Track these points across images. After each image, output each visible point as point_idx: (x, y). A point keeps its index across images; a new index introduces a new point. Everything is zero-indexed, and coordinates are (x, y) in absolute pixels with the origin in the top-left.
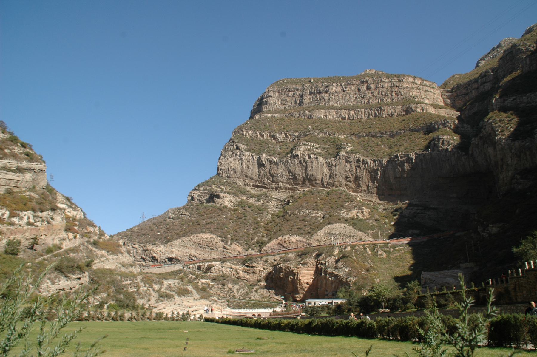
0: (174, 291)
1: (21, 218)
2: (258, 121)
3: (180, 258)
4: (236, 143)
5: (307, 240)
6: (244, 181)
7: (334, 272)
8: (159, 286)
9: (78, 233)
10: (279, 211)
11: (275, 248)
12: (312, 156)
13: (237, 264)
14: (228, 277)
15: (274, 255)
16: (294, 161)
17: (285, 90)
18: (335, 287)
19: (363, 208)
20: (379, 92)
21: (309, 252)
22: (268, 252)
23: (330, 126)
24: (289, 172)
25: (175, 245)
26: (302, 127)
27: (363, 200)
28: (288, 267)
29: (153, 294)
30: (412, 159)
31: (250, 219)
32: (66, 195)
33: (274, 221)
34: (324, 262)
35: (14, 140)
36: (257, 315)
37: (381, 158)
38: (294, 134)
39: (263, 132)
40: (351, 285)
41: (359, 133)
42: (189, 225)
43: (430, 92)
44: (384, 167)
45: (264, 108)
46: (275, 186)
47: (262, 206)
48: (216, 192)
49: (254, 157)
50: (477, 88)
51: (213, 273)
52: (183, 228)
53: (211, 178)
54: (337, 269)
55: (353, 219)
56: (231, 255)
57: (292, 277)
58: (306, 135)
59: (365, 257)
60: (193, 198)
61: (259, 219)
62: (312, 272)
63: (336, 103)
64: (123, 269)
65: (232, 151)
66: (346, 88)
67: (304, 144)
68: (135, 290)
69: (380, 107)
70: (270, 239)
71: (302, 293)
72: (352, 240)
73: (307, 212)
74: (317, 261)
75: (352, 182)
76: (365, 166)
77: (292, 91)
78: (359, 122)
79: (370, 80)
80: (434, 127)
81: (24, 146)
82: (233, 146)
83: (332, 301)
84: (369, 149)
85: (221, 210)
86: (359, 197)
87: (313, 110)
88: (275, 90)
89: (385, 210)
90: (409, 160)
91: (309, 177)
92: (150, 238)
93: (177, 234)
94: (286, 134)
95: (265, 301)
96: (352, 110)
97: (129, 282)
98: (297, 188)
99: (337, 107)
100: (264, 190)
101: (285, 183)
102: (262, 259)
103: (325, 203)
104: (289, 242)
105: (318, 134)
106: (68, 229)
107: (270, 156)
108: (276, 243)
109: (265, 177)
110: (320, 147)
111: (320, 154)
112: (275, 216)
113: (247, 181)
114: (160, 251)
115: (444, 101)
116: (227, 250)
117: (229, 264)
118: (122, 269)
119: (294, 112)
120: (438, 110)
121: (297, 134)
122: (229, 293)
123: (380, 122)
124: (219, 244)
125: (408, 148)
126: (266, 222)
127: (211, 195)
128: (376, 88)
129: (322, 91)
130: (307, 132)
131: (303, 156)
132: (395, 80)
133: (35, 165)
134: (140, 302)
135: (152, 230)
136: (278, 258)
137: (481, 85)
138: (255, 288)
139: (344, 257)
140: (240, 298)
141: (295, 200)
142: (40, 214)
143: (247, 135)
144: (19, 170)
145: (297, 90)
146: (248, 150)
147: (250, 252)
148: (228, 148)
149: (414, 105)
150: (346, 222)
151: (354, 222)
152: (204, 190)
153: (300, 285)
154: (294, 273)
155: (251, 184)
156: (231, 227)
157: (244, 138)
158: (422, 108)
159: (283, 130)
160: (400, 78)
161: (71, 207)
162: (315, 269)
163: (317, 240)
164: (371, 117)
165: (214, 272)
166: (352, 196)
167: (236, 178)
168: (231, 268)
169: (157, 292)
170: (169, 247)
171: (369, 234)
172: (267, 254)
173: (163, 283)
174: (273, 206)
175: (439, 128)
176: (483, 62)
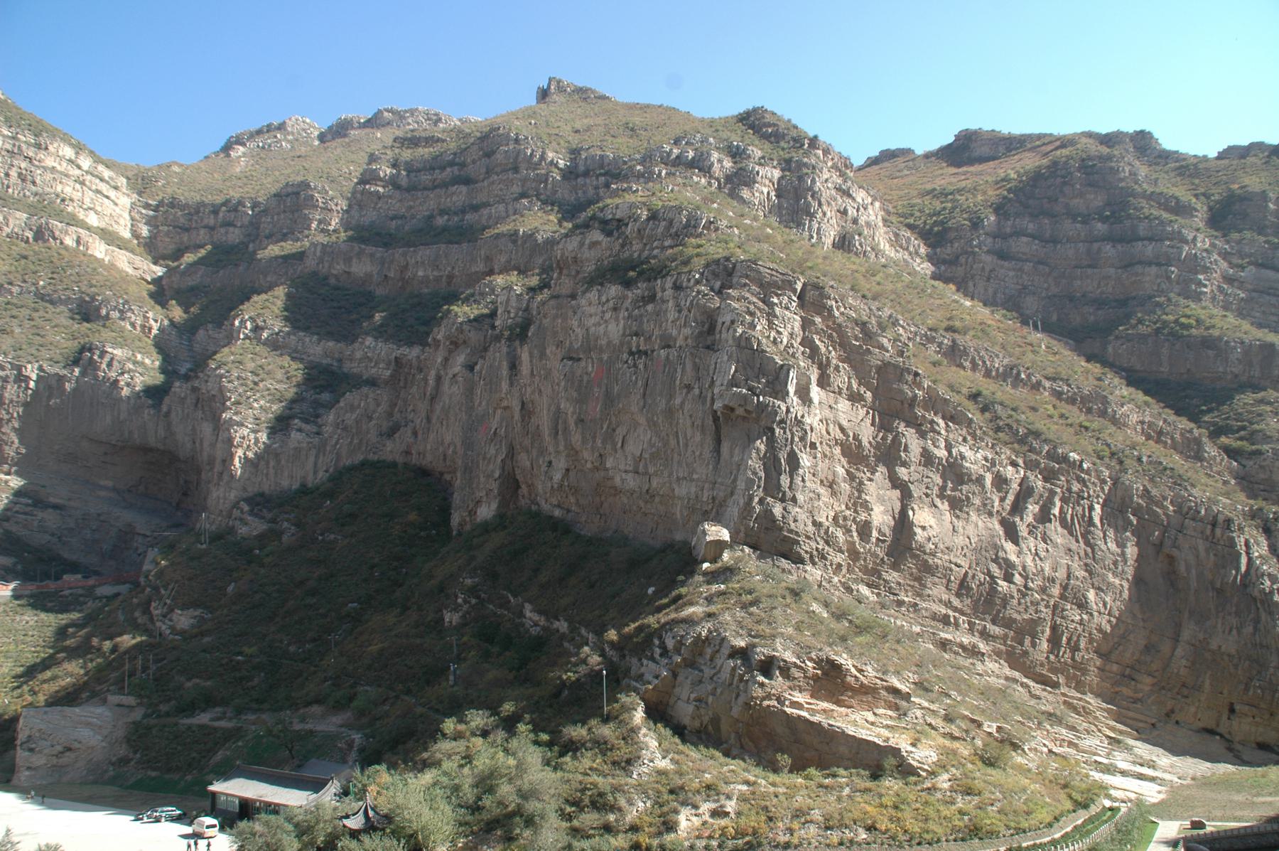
30: (28, 378)
43: (107, 197)
50: (212, 229)
80: (98, 309)
90: (21, 379)
115: (132, 225)
120: (113, 251)
125: (24, 347)
137: (221, 226)
158: (79, 237)
175: (107, 317)
176: (241, 149)
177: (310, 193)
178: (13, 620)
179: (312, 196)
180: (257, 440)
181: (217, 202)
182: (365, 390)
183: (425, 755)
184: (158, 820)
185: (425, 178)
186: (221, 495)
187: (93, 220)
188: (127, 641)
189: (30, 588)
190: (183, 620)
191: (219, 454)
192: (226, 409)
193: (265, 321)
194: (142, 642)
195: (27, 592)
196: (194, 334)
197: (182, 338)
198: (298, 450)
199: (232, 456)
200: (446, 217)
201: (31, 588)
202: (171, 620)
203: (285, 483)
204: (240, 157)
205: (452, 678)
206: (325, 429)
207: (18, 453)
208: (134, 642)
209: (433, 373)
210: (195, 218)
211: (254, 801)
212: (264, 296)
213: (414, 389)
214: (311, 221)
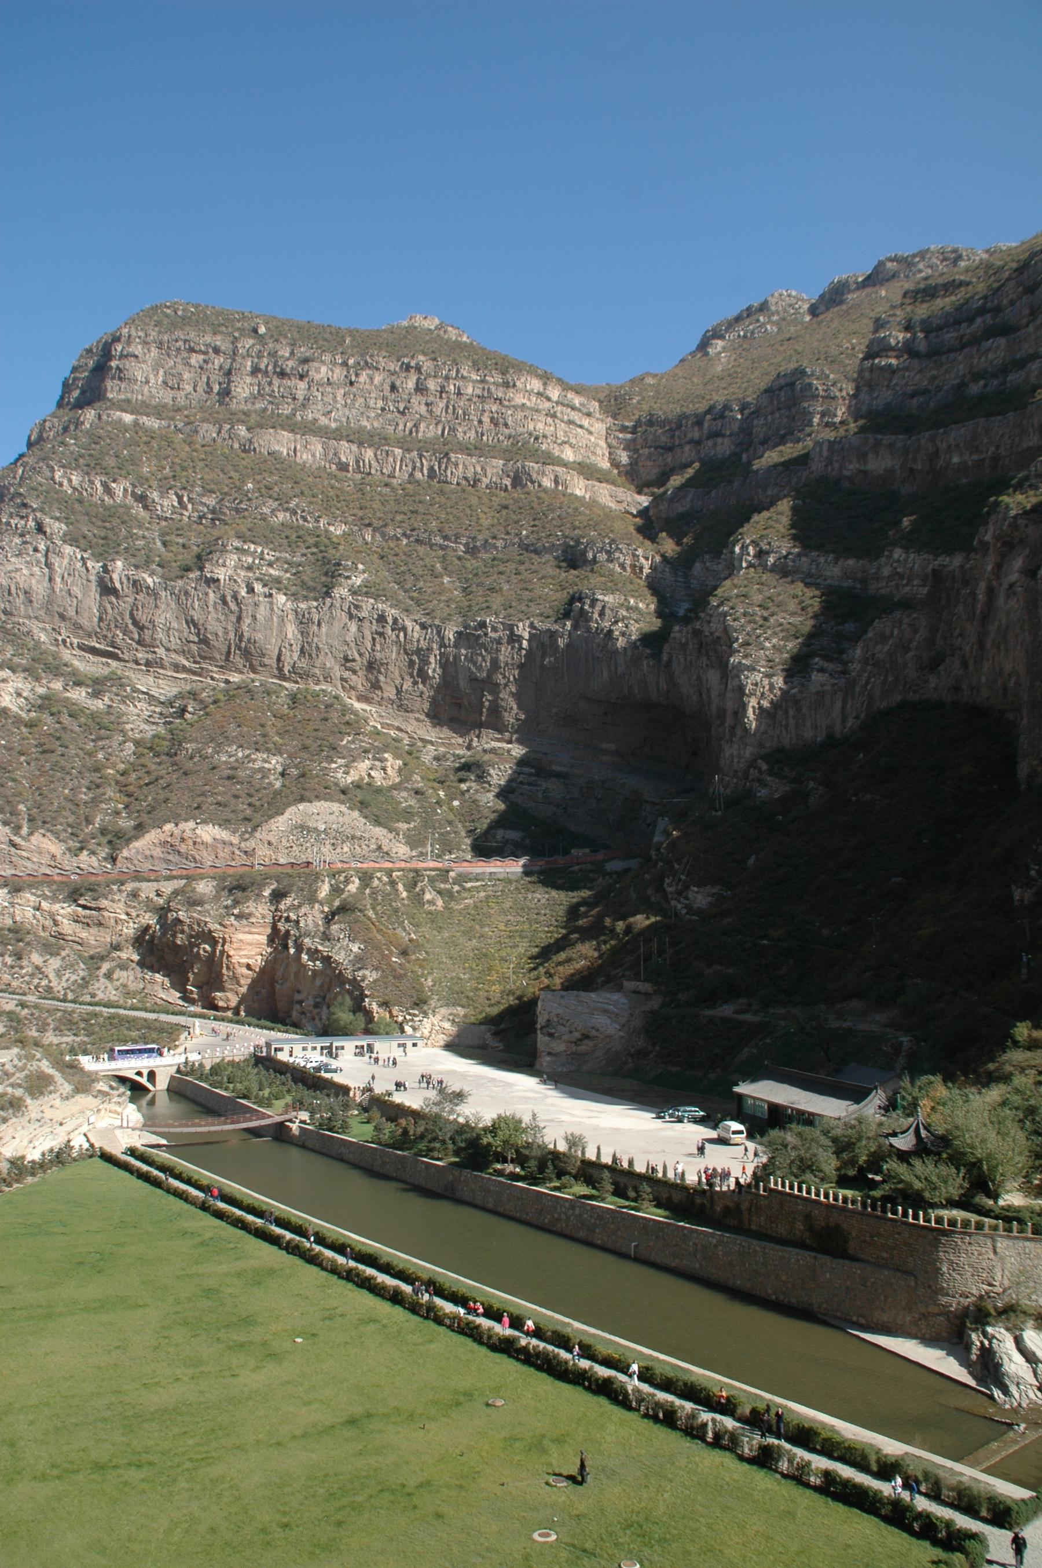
2: (95, 438)
4: (34, 510)
7: (320, 948)
11: (155, 854)
12: (258, 587)
13: (54, 899)
14: (29, 933)
16: (207, 594)
17: (180, 343)
18: (322, 986)
19: (386, 755)
20: (447, 407)
21: (253, 884)
23: (306, 491)
24: (187, 622)
26: (227, 481)
30: (520, 638)
31: (77, 755)
33: (143, 766)
34: (293, 916)
37: (443, 621)
39: (114, 481)
41: (386, 525)
43: (581, 427)
45: (112, 390)
46: (146, 656)
47: (109, 713)
49: (90, 564)
50: (697, 443)
54: (329, 940)
55: (358, 786)
57: (207, 947)
59: (396, 910)
61: (100, 756)
62: (263, 939)
65: (22, 535)
66: (357, 375)
67: (237, 549)
69: (447, 454)
70: (140, 829)
71: (232, 990)
73: (240, 754)
74: (276, 910)
76: (398, 636)
77: (201, 352)
78: (386, 485)
79: (427, 365)
80: (584, 553)
88: (149, 339)
89: (437, 758)
90: (514, 639)
91: (243, 645)
94: (180, 499)
96: (370, 446)
98: (208, 670)
99: (327, 427)
100: (114, 664)
102: (123, 888)
104: (195, 843)
107: (137, 567)
109: (116, 626)
110: (278, 559)
113: (63, 631)
115: (610, 453)
116: (19, 852)
117: (32, 898)
120: (593, 486)
121: (211, 501)
122: (36, 981)
123: (443, 500)
125: (514, 604)
126: (122, 766)
128: (441, 392)
129: (288, 370)
130: (241, 502)
136: (168, 888)
137: (708, 438)
138: (106, 966)
139: (343, 909)
140: (65, 995)
143: (65, 483)
145: (217, 351)
146: (71, 539)
149: (536, 466)
150: (342, 797)
153: (228, 968)
154: (214, 937)
155: (75, 641)
156: (24, 777)
157: (57, 492)
158: (556, 477)
162: (269, 931)
163: (270, 843)
164: (418, 475)
166: (355, 713)
167: (30, 618)
168: (38, 910)
172: (138, 877)
175: (594, 560)
176: (720, 344)
177: (807, 381)
178: (525, 898)
179: (810, 385)
180: (772, 687)
181: (700, 410)
182: (898, 614)
183: (991, 1066)
184: (680, 1120)
185: (949, 336)
186: (735, 753)
187: (569, 455)
188: (641, 921)
189: (540, 863)
190: (700, 898)
191: (730, 705)
192: (733, 652)
193: (769, 544)
194: (656, 922)
195: (537, 868)
196: (690, 568)
197: (676, 575)
198: (821, 694)
199: (744, 706)
200: (982, 383)
201: (540, 864)
202: (687, 898)
203: (808, 735)
204: (720, 353)
205: (1024, 971)
206: (851, 666)
207: (518, 720)
208: (647, 922)
209: (982, 585)
210: (677, 433)
211: (785, 1108)
212: (765, 514)
213: (960, 608)
214: (812, 414)
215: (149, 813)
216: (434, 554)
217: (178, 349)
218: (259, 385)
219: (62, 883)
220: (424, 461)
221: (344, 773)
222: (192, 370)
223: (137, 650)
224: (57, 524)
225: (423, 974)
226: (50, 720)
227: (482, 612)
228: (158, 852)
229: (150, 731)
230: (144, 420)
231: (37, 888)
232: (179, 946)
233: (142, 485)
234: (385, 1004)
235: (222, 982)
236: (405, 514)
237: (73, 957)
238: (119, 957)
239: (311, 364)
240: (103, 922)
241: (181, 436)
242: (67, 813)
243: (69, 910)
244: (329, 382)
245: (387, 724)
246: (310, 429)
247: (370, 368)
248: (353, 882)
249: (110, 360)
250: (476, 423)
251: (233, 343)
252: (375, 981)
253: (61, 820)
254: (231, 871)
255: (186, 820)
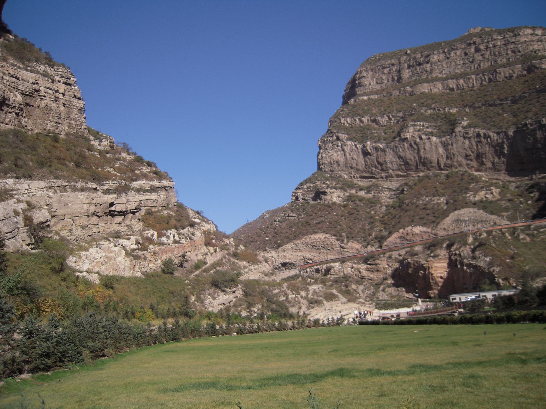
0: (321, 296)
1: (168, 237)
2: (354, 106)
3: (294, 263)
4: (335, 133)
5: (433, 229)
6: (349, 173)
7: (472, 262)
8: (306, 292)
9: (217, 246)
10: (394, 202)
12: (424, 137)
13: (358, 263)
15: (398, 250)
16: (404, 145)
17: (379, 67)
19: (492, 188)
20: (491, 53)
21: (438, 243)
22: (390, 247)
23: (438, 101)
25: (287, 249)
26: (406, 106)
27: (489, 179)
28: (417, 262)
29: (302, 301)
32: (196, 210)
33: (390, 213)
34: (457, 252)
35: (139, 160)
36: (395, 315)
37: (506, 129)
38: (398, 115)
39: (363, 117)
40: (496, 276)
41: (474, 103)
42: (298, 227)
44: (510, 139)
45: (358, 91)
46: (385, 174)
47: (374, 198)
48: (322, 189)
49: (358, 146)
51: (333, 275)
52: (292, 231)
53: (313, 174)
54: (475, 258)
55: (481, 201)
56: (349, 254)
57: (422, 272)
58: (412, 115)
59: (506, 243)
60: (297, 198)
61: (372, 212)
62: (446, 265)
63: (440, 73)
64: (267, 279)
65: (332, 142)
66: (449, 54)
67: (412, 125)
68: (284, 298)
70: (390, 233)
71: (435, 289)
72: (485, 226)
73: (427, 199)
74: (450, 251)
75: (474, 160)
76: (487, 140)
77: (387, 67)
78: (471, 90)
79: (478, 40)
81: (149, 164)
82: (332, 136)
83: (480, 295)
84: (488, 120)
85: (329, 207)
86: (484, 176)
87: (415, 85)
89: (517, 187)
91: (422, 160)
92: (259, 244)
93: (287, 238)
94: (388, 117)
95: (395, 301)
97: (277, 291)
99: (442, 77)
100: (373, 180)
101: (396, 170)
102: (385, 255)
103: (446, 188)
104: (413, 235)
105: (426, 111)
106: (208, 244)
107: (375, 142)
108: (397, 237)
109: (372, 166)
110: (430, 126)
111: (432, 134)
112: (390, 208)
113: (353, 173)
114: (272, 257)
116: (344, 250)
117: (350, 264)
118: (265, 279)
119: (393, 90)
121: (401, 114)
124: (334, 243)
125: (539, 113)
126: (381, 215)
127: (317, 192)
128: (486, 49)
130: (412, 111)
131: (413, 138)
132: (509, 35)
133: (164, 183)
134: (293, 310)
135: (260, 236)
136: (403, 252)
138: (382, 287)
139: (481, 245)
141: (410, 187)
142: (182, 231)
143: (345, 123)
144: (153, 190)
145: (393, 65)
147: (370, 249)
148: (327, 140)
150: (474, 206)
151: (484, 205)
152: (308, 188)
153: (432, 279)
154: (424, 267)
155: (358, 175)
156: (344, 224)
157: (343, 126)
159: (384, 112)
160: (515, 31)
161: (204, 221)
162: (448, 261)
163: (444, 229)
164: (484, 83)
165: (334, 273)
166: (476, 176)
167: (340, 171)
169: (305, 298)
170: (281, 252)
171: (503, 217)
172: (390, 250)
173: (308, 288)
174: (386, 197)
215: (393, 227)
216: (497, 108)
217: (379, 69)
218: (412, 71)
219: (361, 257)
220: (486, 77)
221: (473, 197)
222: (386, 75)
223: (381, 173)
224: (344, 135)
225: (524, 266)
226: (351, 203)
227: (524, 120)
228: (398, 241)
229: (391, 201)
230: (372, 97)
231: (351, 260)
232: (409, 273)
233: (373, 116)
234: (506, 279)
235: (431, 286)
236: (481, 97)
237: (368, 285)
238: (387, 283)
239: (430, 57)
240: (379, 269)
241: (386, 98)
242: (361, 233)
243: (365, 266)
244: (439, 61)
245: (491, 178)
246: (437, 79)
247: (454, 50)
248: (483, 235)
249: (355, 81)
250: (505, 55)
251: (398, 60)
252: (499, 271)
253: (359, 236)
254: (429, 241)
255: (408, 226)
